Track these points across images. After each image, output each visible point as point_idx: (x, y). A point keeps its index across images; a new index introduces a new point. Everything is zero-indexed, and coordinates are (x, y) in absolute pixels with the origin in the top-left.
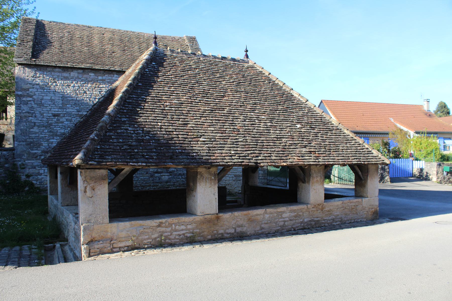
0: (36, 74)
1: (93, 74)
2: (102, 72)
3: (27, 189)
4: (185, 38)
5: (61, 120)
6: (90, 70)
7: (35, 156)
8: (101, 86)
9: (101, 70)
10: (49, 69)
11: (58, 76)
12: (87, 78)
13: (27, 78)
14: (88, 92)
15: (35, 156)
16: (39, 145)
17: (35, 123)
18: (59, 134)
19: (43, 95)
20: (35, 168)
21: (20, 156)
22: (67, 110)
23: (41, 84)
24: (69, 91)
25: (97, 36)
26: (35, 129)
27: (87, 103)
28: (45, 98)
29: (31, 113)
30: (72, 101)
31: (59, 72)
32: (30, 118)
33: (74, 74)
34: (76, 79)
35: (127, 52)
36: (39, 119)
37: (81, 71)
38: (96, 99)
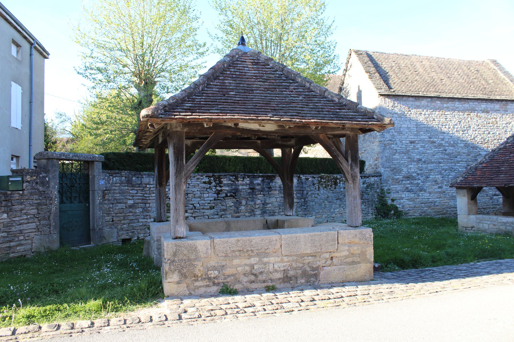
0: (394, 103)
1: (439, 102)
2: (446, 100)
3: (392, 212)
4: (488, 61)
5: (417, 147)
6: (436, 99)
7: (398, 181)
8: (446, 113)
9: (445, 98)
10: (404, 98)
11: (412, 105)
12: (435, 106)
13: (387, 108)
14: (436, 119)
15: (398, 181)
16: (400, 171)
17: (396, 150)
18: (415, 160)
19: (401, 123)
20: (398, 193)
21: (386, 181)
22: (421, 137)
23: (399, 113)
24: (421, 118)
25: (418, 64)
26: (397, 156)
27: (436, 130)
28: (403, 126)
29: (392, 141)
30: (423, 129)
31: (412, 101)
32: (393, 145)
33: (424, 102)
34: (426, 107)
35: (452, 79)
36: (400, 146)
37: (429, 100)
38: (442, 125)
